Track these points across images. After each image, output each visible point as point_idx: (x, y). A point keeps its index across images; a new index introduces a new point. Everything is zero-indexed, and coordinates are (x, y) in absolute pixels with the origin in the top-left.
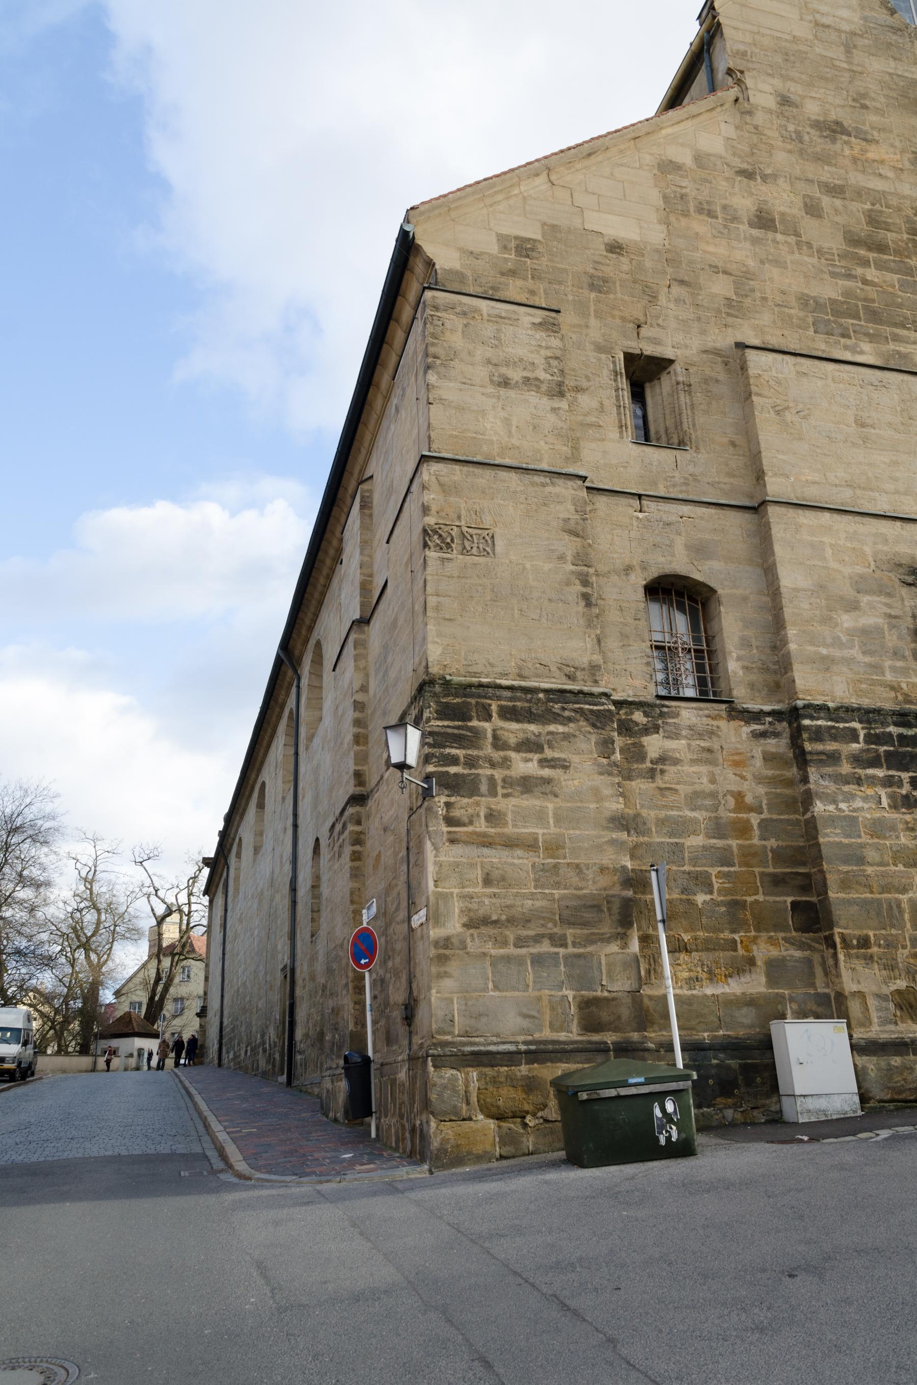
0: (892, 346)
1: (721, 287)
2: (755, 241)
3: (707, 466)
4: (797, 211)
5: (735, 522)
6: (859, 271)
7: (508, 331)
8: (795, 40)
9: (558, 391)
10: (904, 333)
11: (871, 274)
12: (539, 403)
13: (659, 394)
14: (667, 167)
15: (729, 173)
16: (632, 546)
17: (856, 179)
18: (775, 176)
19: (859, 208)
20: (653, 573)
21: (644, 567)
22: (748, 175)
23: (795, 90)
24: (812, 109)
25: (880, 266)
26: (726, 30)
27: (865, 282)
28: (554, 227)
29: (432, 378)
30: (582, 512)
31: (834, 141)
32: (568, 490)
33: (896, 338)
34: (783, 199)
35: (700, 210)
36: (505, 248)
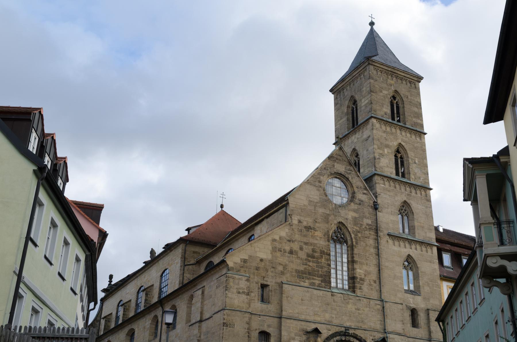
0: (312, 281)
1: (280, 268)
2: (289, 257)
3: (271, 308)
4: (298, 250)
5: (276, 319)
6: (308, 263)
7: (241, 281)
8: (304, 205)
9: (248, 294)
10: (315, 277)
11: (311, 264)
12: (244, 296)
13: (266, 290)
14: (274, 240)
15: (285, 241)
16: (257, 325)
17: (312, 241)
18: (295, 241)
19: (311, 248)
20: (260, 330)
21: (259, 329)
22: (289, 241)
23: (302, 218)
24: (305, 224)
25: (313, 262)
26: (290, 204)
27: (309, 266)
28: (251, 256)
29: (227, 292)
30: (250, 319)
31: (308, 231)
32: (247, 315)
33: (313, 279)
34: (295, 247)
35: (279, 250)
36: (241, 261)
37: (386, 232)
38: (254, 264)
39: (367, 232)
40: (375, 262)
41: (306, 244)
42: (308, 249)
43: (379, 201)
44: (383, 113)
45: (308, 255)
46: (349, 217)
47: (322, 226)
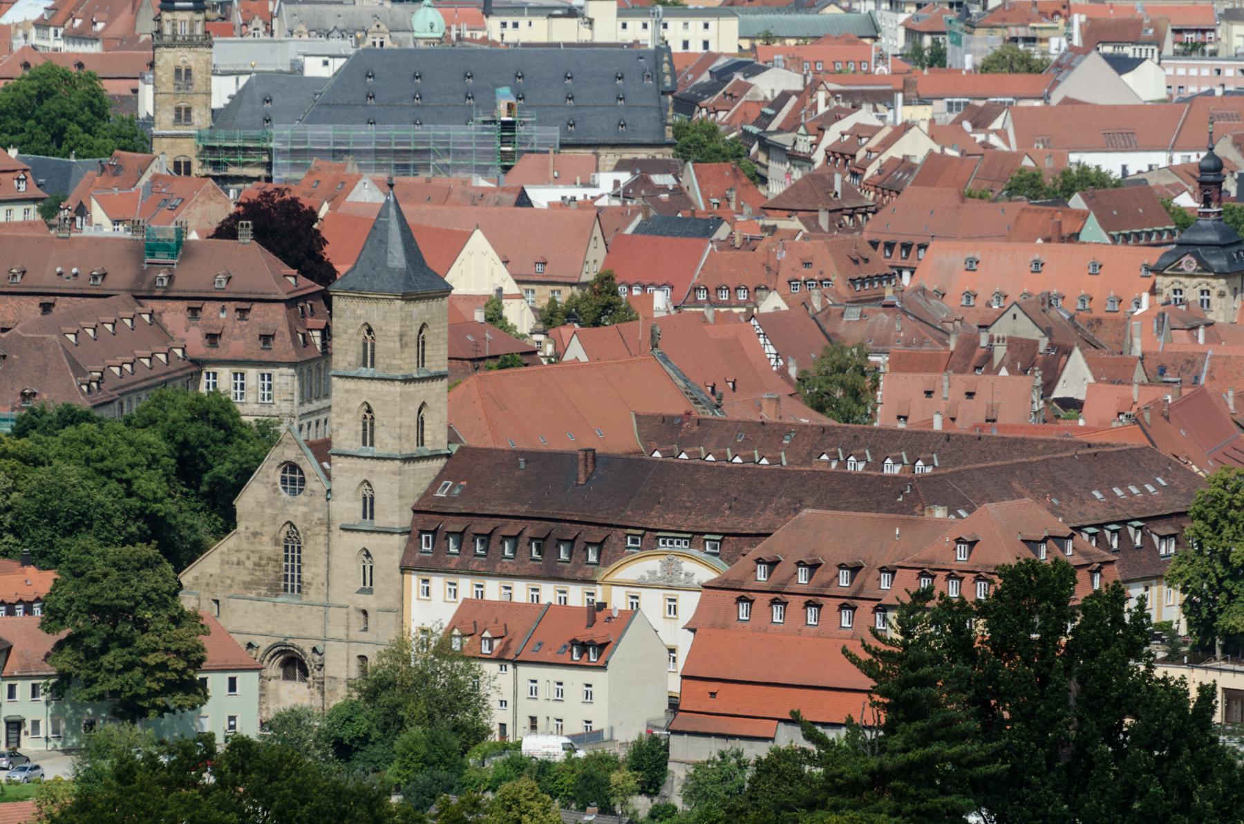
1: (228, 582)
14: (222, 553)
17: (259, 547)
24: (252, 530)
34: (243, 556)
37: (339, 524)
38: (205, 581)
39: (317, 529)
40: (325, 562)
41: (253, 552)
42: (254, 558)
43: (334, 486)
44: (345, 364)
45: (255, 564)
46: (299, 514)
47: (270, 530)
